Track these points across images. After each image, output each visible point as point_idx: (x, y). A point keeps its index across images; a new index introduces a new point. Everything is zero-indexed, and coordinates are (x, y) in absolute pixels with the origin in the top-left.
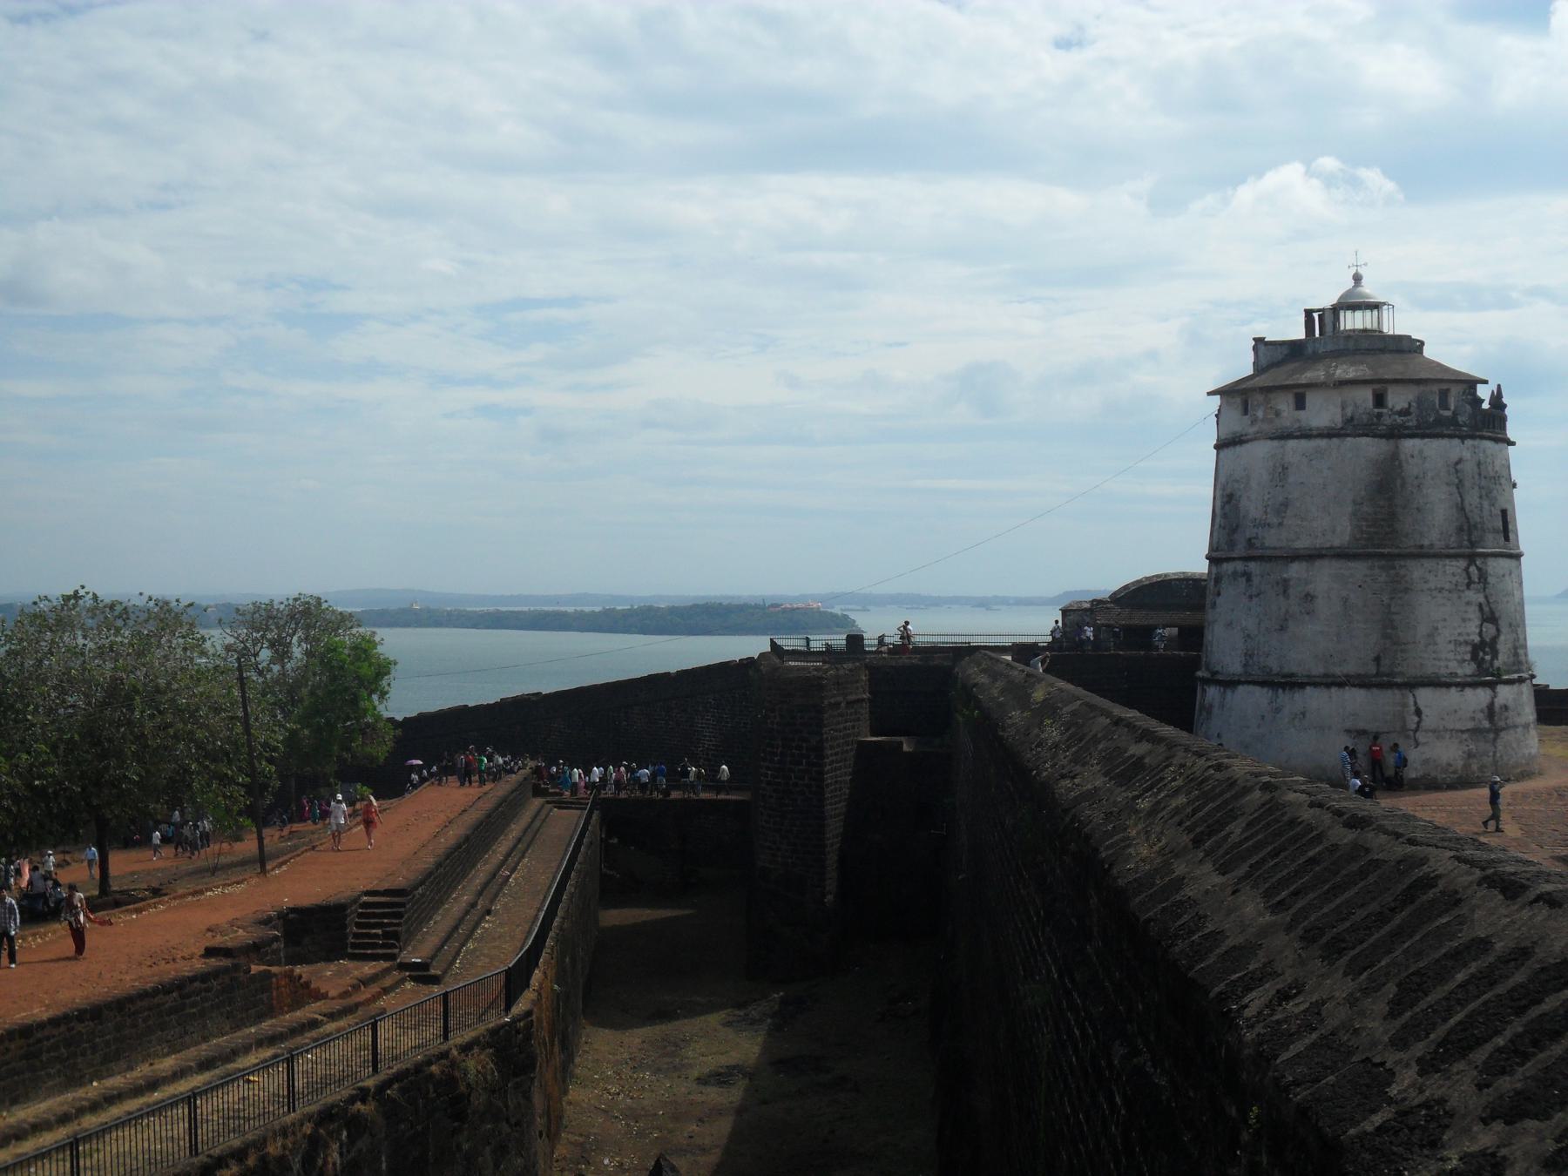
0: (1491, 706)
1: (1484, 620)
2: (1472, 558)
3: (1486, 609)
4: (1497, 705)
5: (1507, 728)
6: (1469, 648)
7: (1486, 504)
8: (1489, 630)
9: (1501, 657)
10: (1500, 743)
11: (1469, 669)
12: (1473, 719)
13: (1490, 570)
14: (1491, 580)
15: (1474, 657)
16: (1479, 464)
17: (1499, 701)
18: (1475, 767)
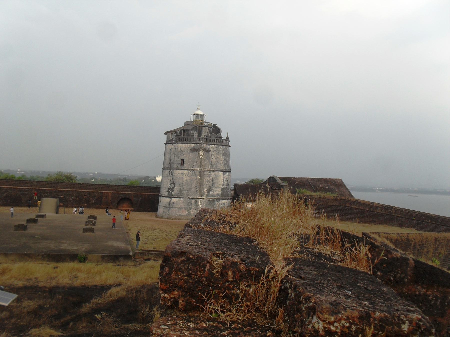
1: (171, 183)
2: (170, 169)
3: (172, 181)
7: (176, 158)
10: (170, 211)
11: (167, 194)
13: (174, 172)
15: (168, 191)
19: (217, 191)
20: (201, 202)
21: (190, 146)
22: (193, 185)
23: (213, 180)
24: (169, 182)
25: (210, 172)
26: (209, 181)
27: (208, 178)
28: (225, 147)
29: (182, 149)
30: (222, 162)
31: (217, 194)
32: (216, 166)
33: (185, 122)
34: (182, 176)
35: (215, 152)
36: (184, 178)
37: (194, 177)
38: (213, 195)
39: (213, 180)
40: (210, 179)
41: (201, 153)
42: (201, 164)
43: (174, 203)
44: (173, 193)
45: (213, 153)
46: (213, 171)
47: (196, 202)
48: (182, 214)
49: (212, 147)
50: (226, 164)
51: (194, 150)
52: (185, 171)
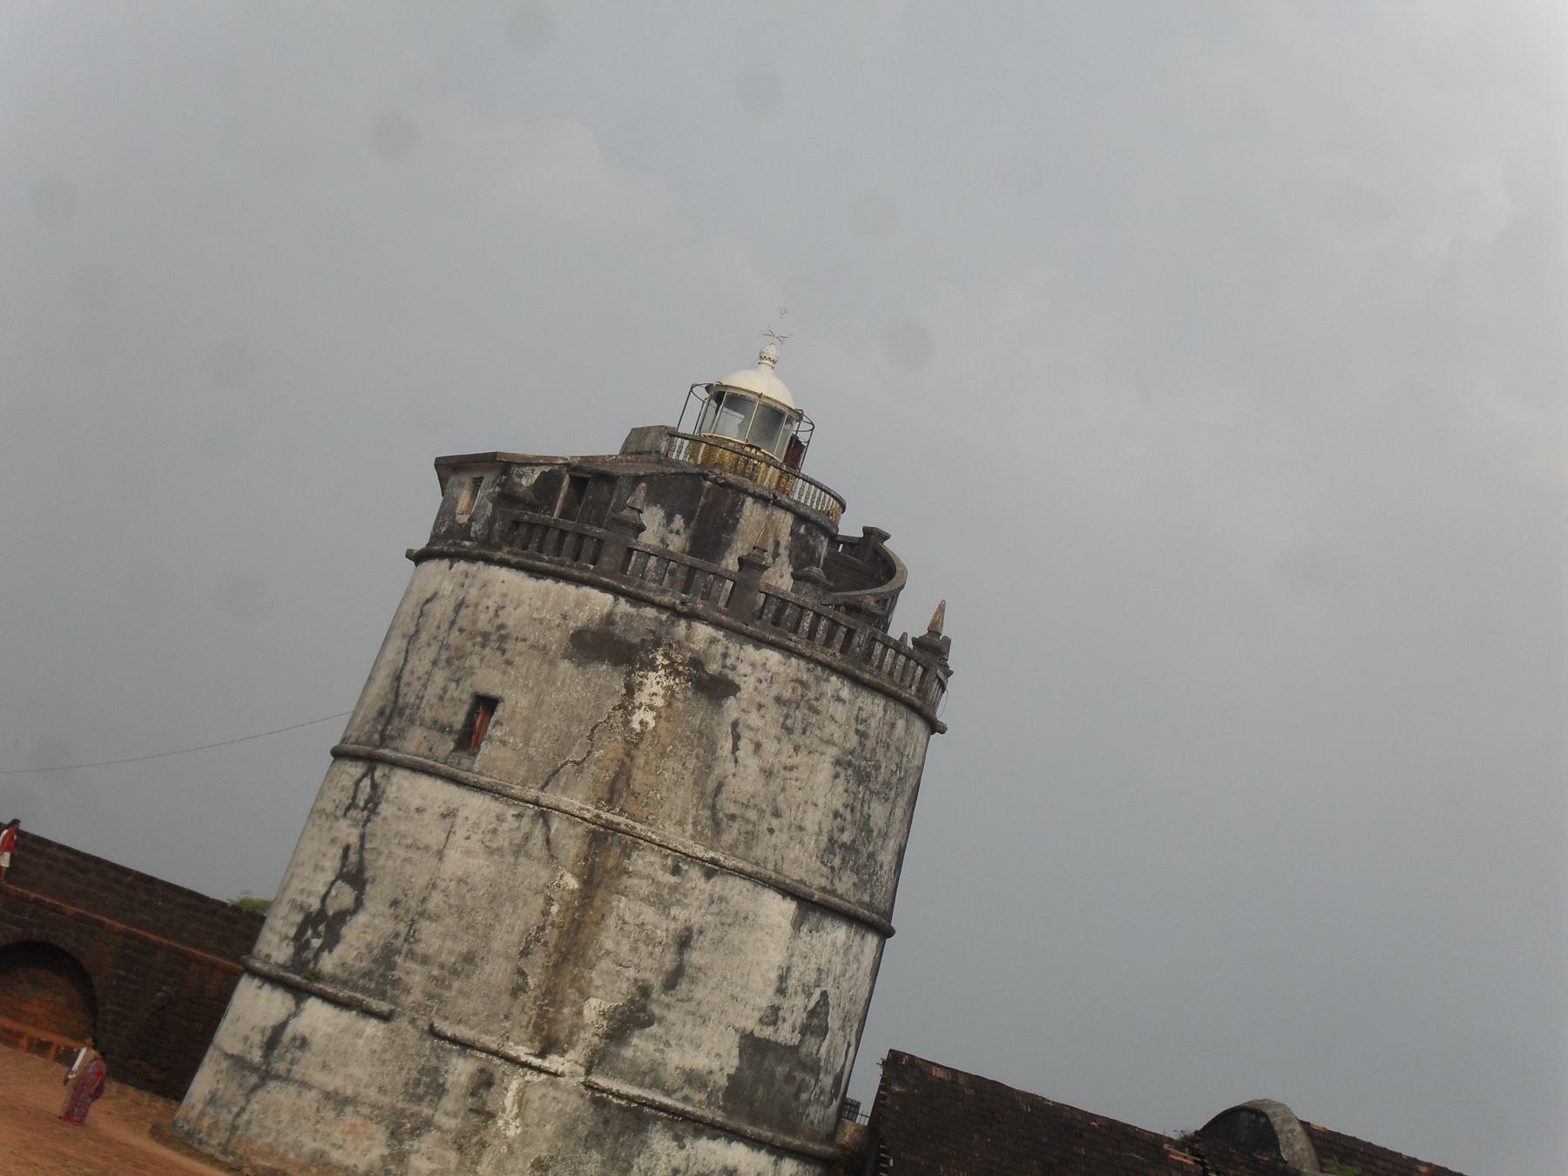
0: (279, 1029)
2: (372, 761)
3: (353, 857)
4: (289, 1032)
5: (286, 1079)
6: (299, 918)
7: (440, 677)
8: (344, 896)
9: (339, 950)
12: (246, 1038)
13: (391, 792)
14: (385, 809)
16: (460, 605)
17: (298, 1026)
18: (207, 1121)
19: (698, 1047)
20: (521, 1102)
21: (579, 604)
22: (506, 937)
23: (684, 941)
24: (331, 864)
25: (679, 862)
26: (650, 941)
27: (650, 915)
28: (875, 706)
29: (511, 618)
30: (811, 820)
31: (693, 1078)
32: (751, 837)
33: (638, 434)
34: (435, 836)
35: (773, 711)
36: (452, 855)
37: (533, 872)
38: (651, 1075)
39: (684, 941)
40: (664, 928)
41: (654, 686)
42: (623, 773)
43: (303, 1043)
44: (328, 963)
45: (754, 719)
46: (712, 870)
47: (485, 1081)
48: (336, 1156)
49: (760, 669)
50: (850, 849)
51: (594, 645)
52: (476, 806)
